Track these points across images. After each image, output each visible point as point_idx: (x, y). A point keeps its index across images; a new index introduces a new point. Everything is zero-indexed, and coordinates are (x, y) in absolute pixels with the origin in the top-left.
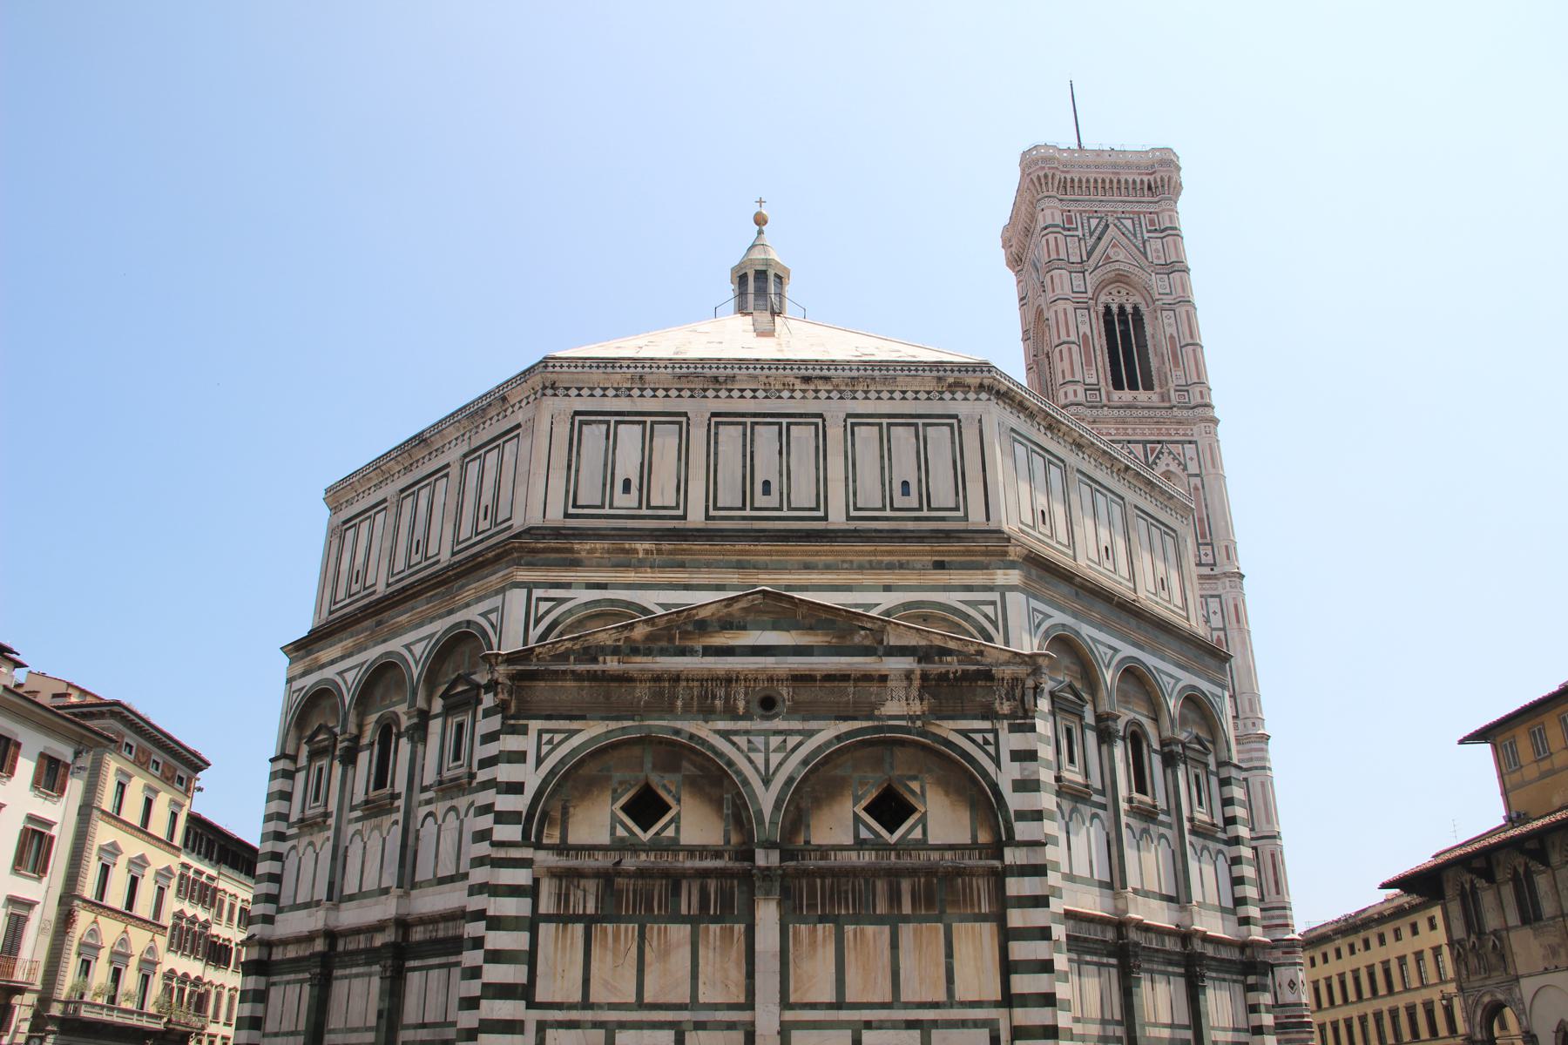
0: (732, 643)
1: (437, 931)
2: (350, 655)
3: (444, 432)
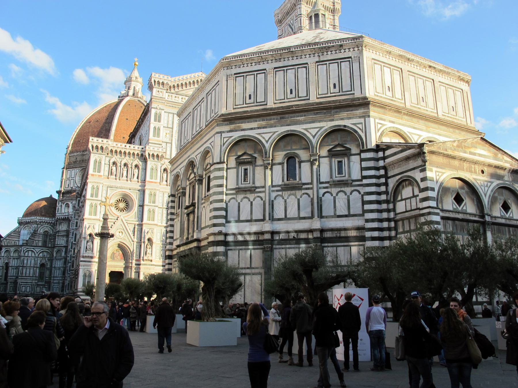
0: (475, 152)
1: (340, 234)
2: (264, 128)
3: (304, 51)
